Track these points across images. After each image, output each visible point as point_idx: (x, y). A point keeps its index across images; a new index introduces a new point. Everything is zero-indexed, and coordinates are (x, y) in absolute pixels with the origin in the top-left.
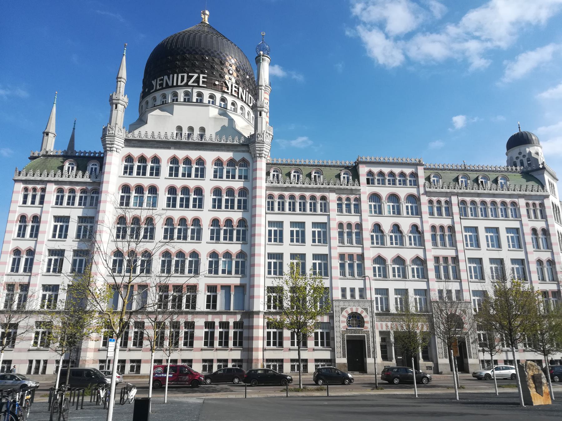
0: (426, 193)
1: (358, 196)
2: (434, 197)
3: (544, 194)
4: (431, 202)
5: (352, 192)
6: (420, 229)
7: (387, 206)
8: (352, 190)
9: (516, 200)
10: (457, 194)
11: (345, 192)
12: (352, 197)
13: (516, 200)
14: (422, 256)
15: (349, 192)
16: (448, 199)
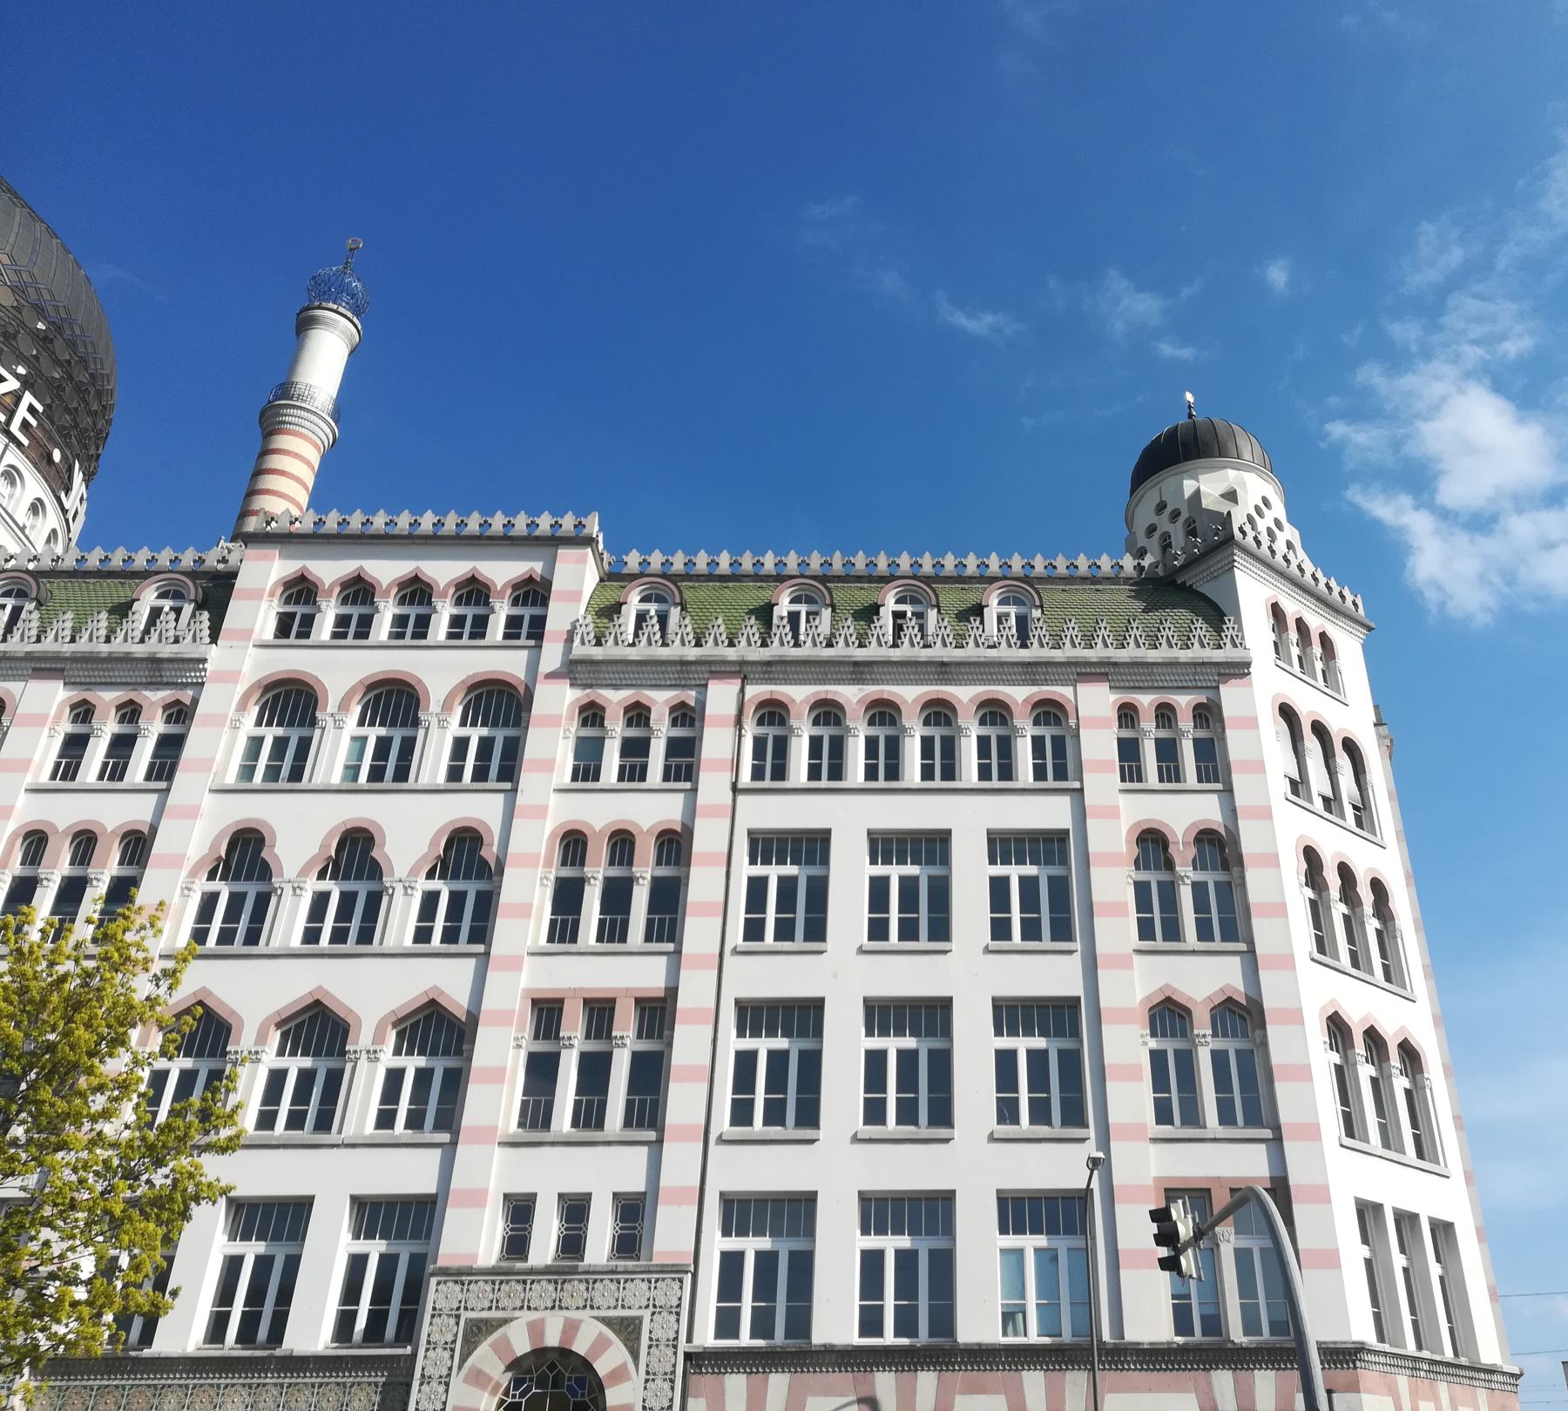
0: (573, 670)
1: (186, 696)
2: (616, 687)
3: (1226, 654)
4: (592, 714)
5: (156, 670)
6: (489, 852)
7: (340, 739)
8: (154, 661)
9: (1063, 692)
10: (743, 672)
11: (118, 674)
12: (155, 698)
13: (1063, 692)
14: (457, 997)
15: (141, 674)
16: (690, 696)
